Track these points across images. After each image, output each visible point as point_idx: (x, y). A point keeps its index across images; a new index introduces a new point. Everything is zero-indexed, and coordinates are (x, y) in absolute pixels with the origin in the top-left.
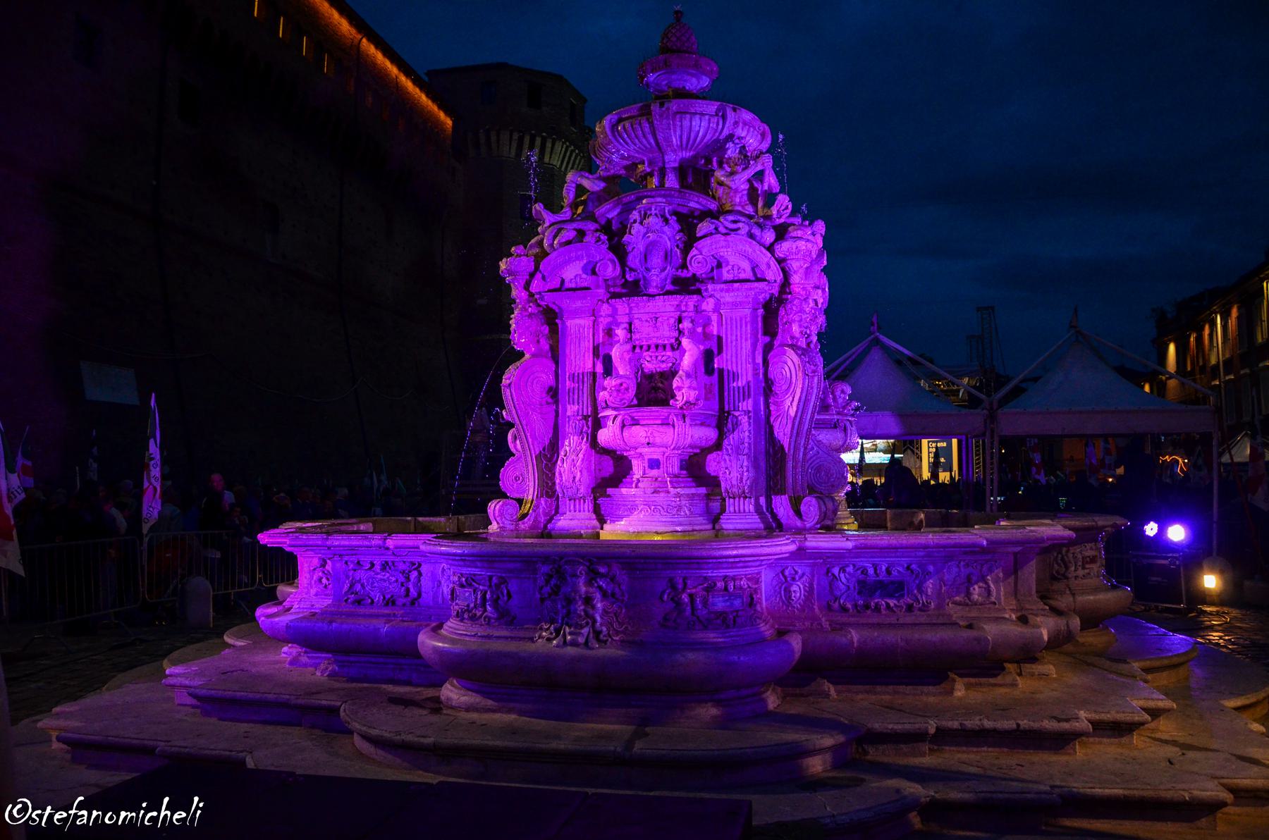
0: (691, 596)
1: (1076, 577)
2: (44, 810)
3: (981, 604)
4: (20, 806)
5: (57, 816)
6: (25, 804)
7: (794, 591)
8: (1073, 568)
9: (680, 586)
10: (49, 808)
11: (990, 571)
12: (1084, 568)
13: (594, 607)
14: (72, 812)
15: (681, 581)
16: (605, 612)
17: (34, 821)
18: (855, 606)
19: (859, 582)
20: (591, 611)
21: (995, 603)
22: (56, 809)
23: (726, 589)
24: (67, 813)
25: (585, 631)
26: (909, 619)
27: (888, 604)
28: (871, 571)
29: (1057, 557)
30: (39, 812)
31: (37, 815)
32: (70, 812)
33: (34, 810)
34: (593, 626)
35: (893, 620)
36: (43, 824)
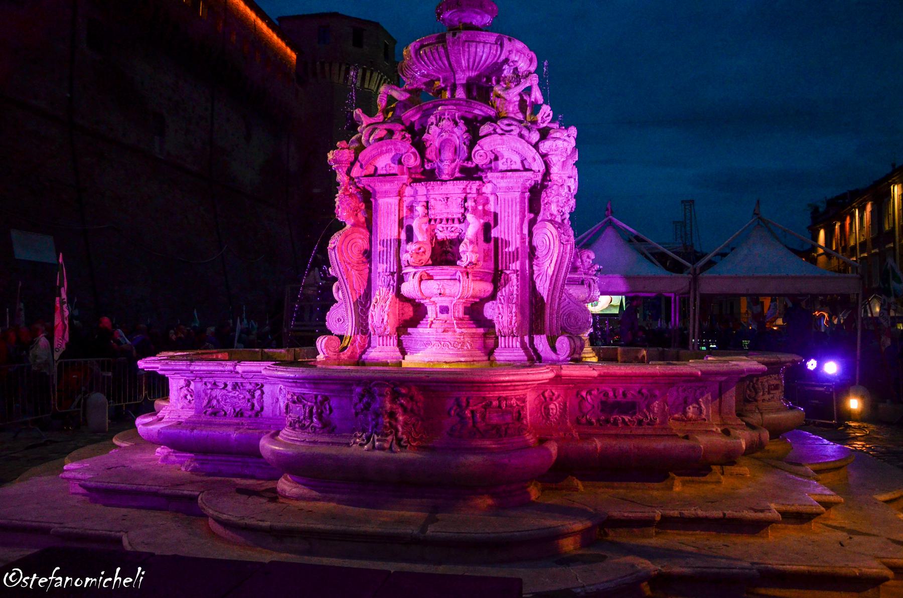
0: (472, 412)
1: (764, 400)
3: (695, 420)
7: (552, 409)
8: (761, 393)
9: (464, 404)
11: (702, 395)
12: (769, 393)
13: (396, 420)
15: (465, 400)
16: (405, 424)
18: (598, 420)
19: (603, 403)
20: (393, 423)
21: (705, 420)
23: (500, 406)
25: (389, 438)
26: (640, 431)
27: (623, 419)
28: (611, 394)
29: (749, 384)
34: (396, 434)
35: (628, 432)
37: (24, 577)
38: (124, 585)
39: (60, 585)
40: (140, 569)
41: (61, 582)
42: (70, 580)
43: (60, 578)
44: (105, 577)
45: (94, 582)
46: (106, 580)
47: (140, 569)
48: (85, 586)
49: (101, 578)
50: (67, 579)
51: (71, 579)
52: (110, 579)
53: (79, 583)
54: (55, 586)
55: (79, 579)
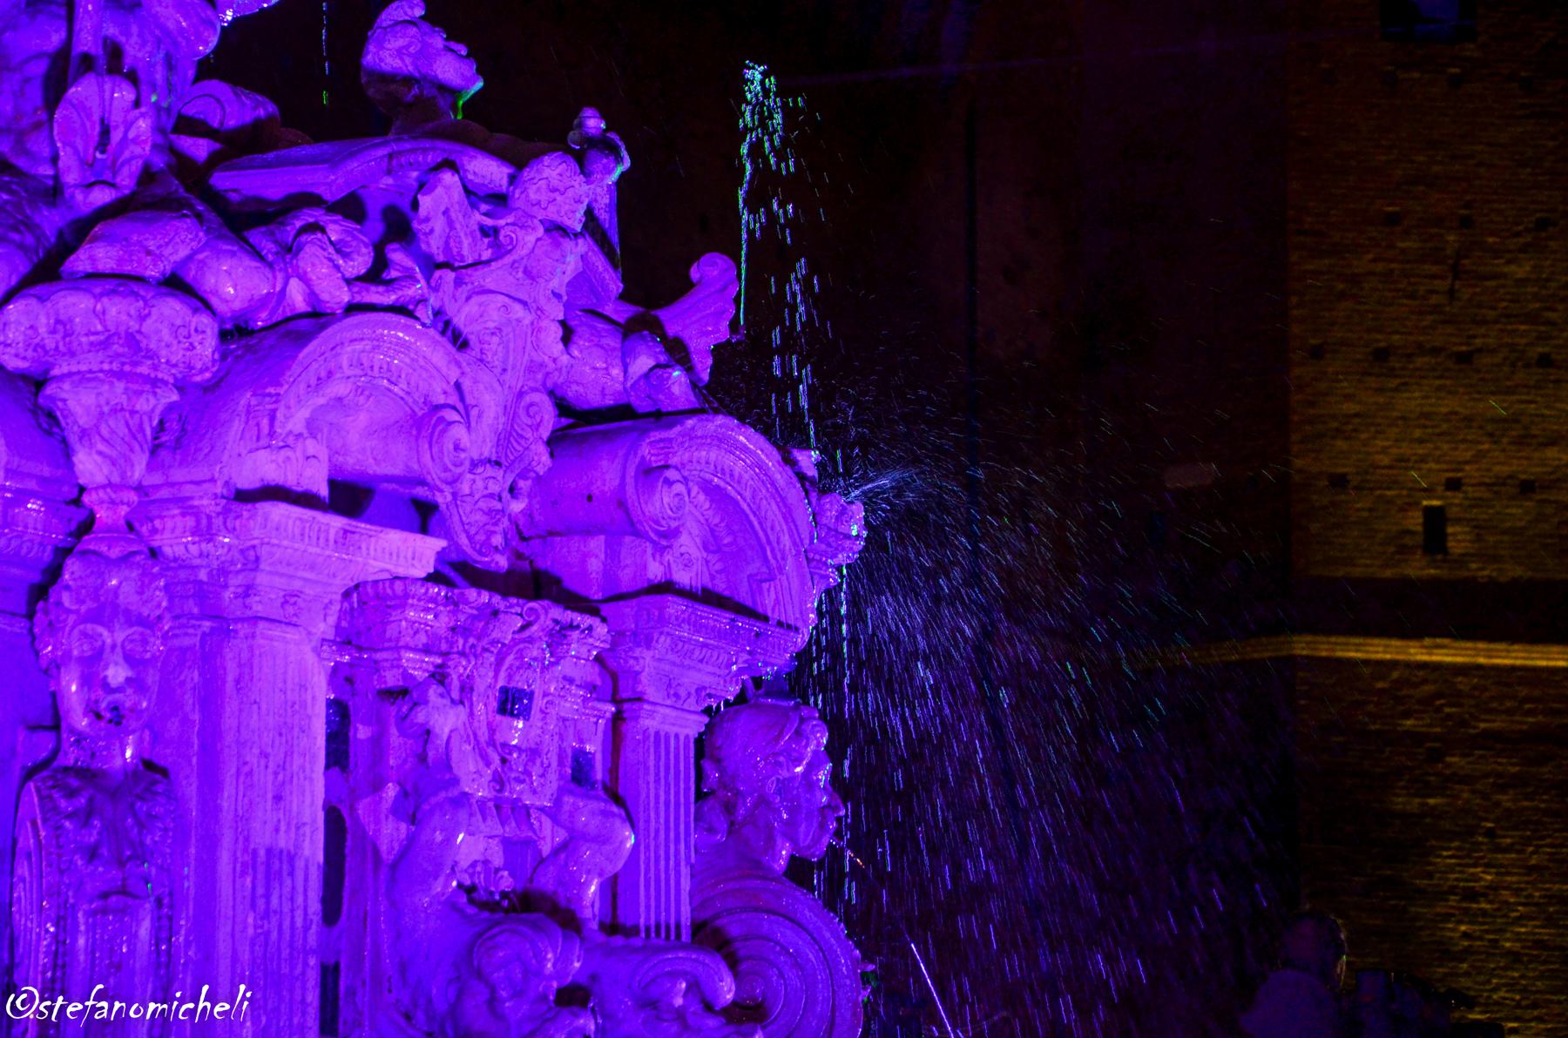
2: (54, 1001)
4: (24, 996)
5: (70, 1009)
6: (31, 994)
10: (61, 998)
14: (89, 1003)
17: (42, 1014)
22: (69, 1000)
24: (83, 1004)
30: (49, 1003)
31: (45, 1007)
32: (86, 1003)
33: (42, 1000)
36: (53, 1018)
37: (41, 1001)
38: (216, 1015)
39: (105, 1015)
40: (242, 987)
41: (105, 1011)
42: (122, 1007)
43: (105, 1004)
44: (182, 1001)
45: (164, 1009)
46: (184, 1007)
47: (242, 987)
48: (148, 1016)
49: (176, 1003)
50: (117, 1005)
51: (124, 1004)
52: (191, 1006)
53: (137, 1012)
54: (96, 1017)
55: (136, 1005)
